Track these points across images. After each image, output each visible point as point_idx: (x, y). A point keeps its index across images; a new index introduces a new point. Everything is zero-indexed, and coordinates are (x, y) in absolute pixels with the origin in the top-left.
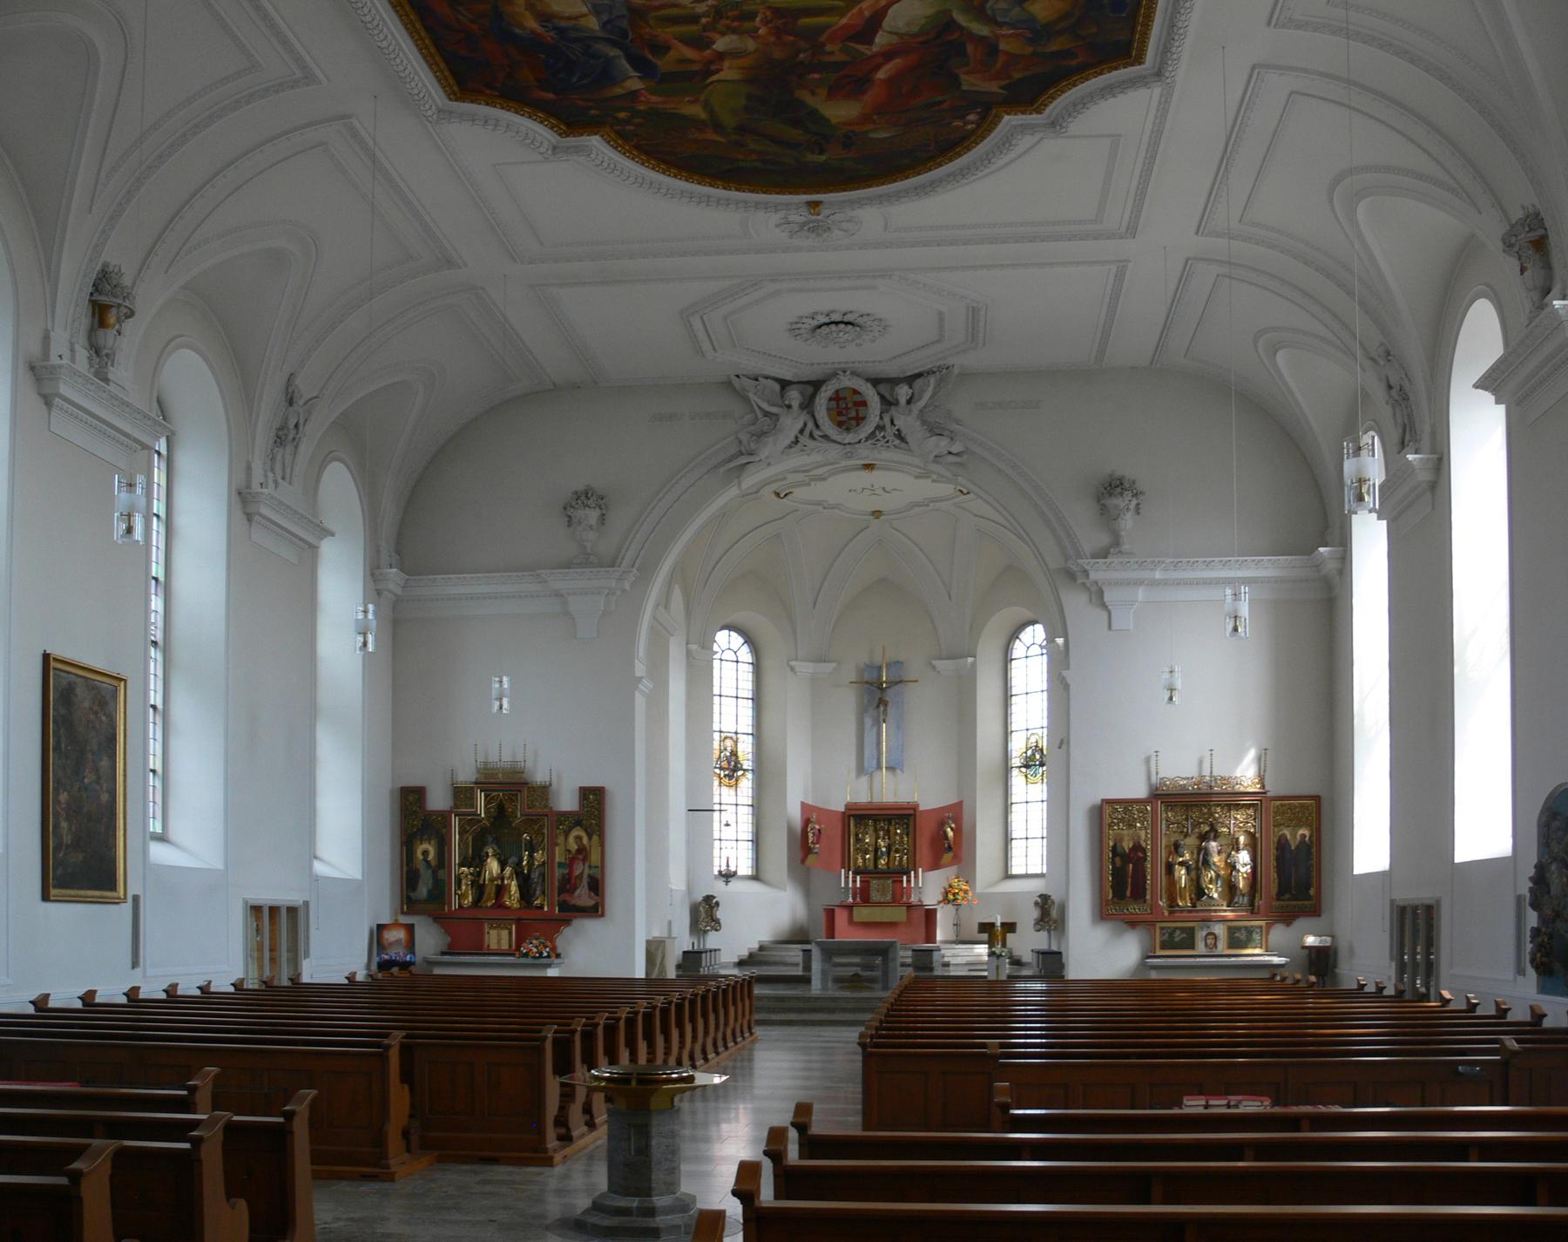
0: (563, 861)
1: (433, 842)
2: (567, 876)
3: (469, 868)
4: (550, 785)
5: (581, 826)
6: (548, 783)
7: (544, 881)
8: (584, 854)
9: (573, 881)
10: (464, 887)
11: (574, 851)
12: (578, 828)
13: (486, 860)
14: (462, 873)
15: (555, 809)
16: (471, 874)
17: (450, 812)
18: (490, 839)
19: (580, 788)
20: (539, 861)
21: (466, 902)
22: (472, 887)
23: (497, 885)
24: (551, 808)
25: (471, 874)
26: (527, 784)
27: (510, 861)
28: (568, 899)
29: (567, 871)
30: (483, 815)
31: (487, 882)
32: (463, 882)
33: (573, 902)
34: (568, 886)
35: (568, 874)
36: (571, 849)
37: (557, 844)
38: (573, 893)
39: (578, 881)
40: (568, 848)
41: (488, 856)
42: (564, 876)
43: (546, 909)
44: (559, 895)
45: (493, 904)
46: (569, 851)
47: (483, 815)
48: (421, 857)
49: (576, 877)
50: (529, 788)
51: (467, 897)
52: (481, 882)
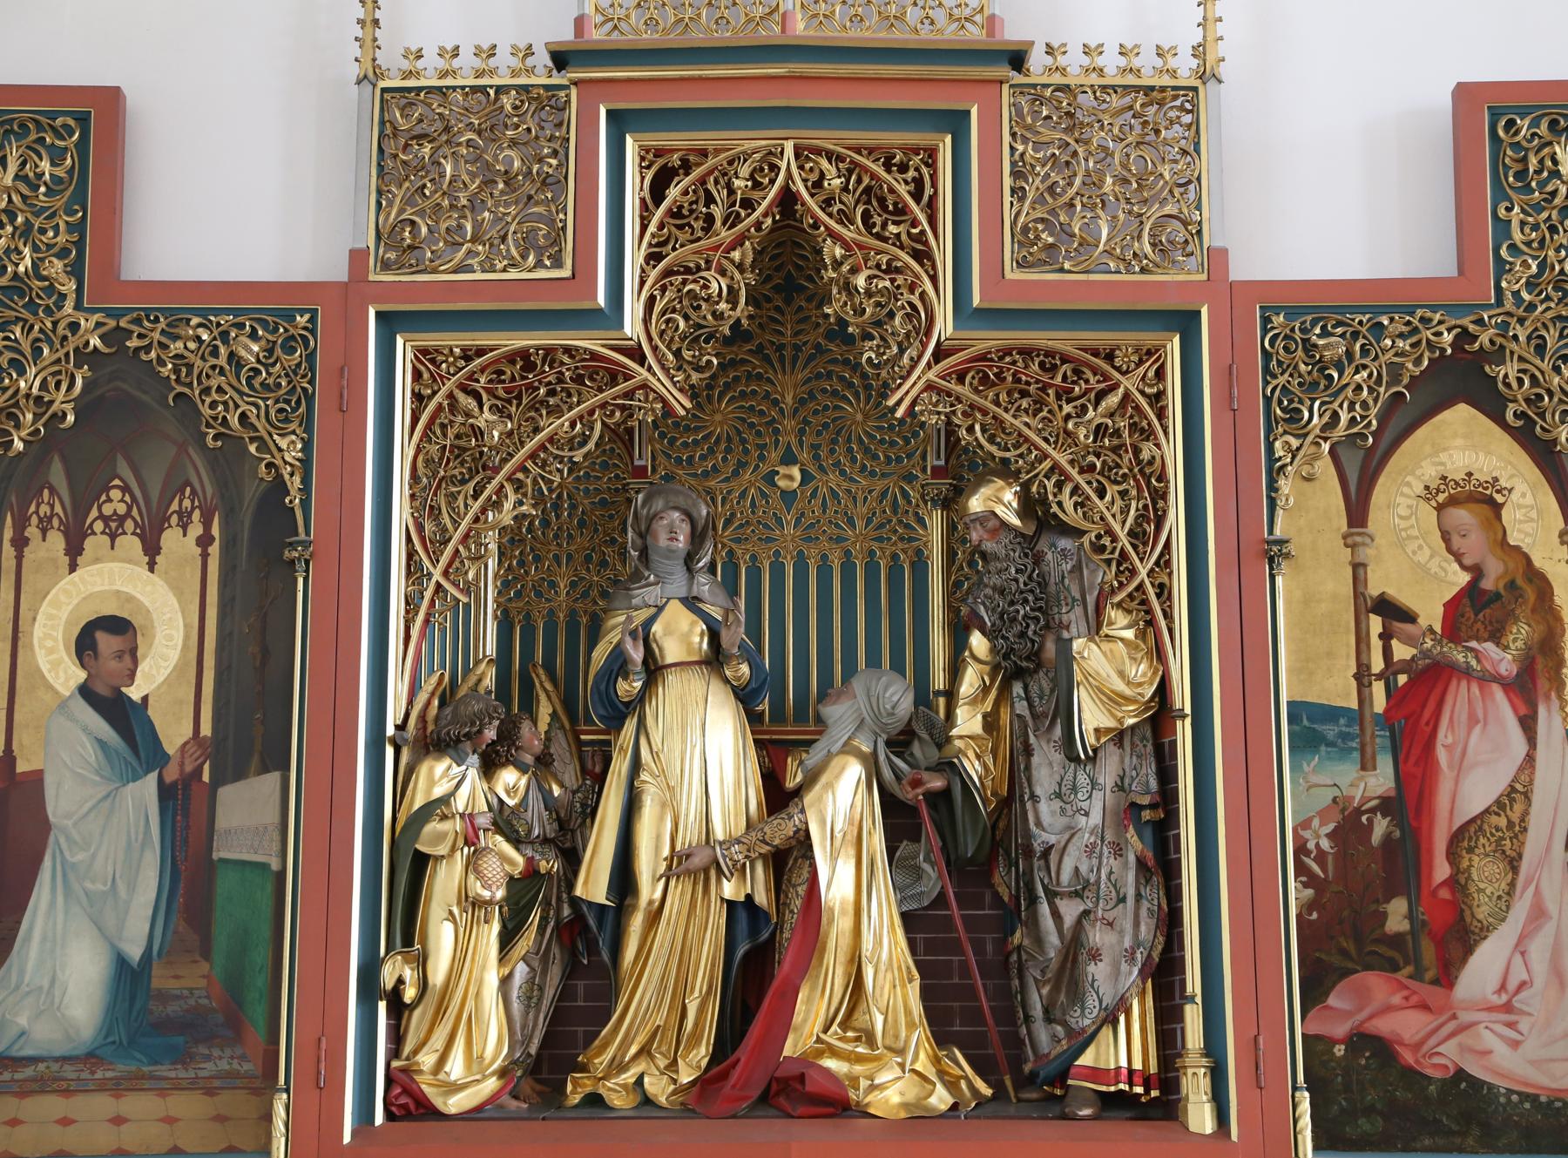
0: (1339, 690)
1: (178, 543)
2: (1381, 826)
3: (489, 768)
4: (1207, 75)
5: (1491, 403)
6: (1185, 65)
7: (1162, 866)
8: (1521, 633)
9: (1442, 871)
10: (442, 939)
11: (1431, 614)
12: (1461, 415)
13: (638, 703)
14: (438, 807)
15: (1242, 269)
16: (505, 822)
17: (354, 289)
18: (673, 532)
19: (1465, 94)
20: (1113, 700)
21: (456, 1068)
22: (507, 940)
23: (742, 912)
24: (1218, 259)
25: (505, 822)
26: (1017, 59)
27: (840, 714)
28: (1404, 1026)
29: (1382, 780)
30: (632, 324)
31: (648, 889)
32: (445, 882)
33: (1450, 1054)
34: (1397, 915)
35: (1386, 806)
36: (1405, 596)
37: (1275, 553)
38: (1447, 977)
39: (1485, 872)
40: (1374, 590)
41: (654, 670)
42: (1350, 825)
43: (1201, 1118)
44: (1315, 990)
45: (708, 1082)
46: (1388, 609)
47: (632, 324)
48: (66, 675)
49: (1461, 838)
50: (1035, 93)
51: (472, 1023)
52: (594, 885)
